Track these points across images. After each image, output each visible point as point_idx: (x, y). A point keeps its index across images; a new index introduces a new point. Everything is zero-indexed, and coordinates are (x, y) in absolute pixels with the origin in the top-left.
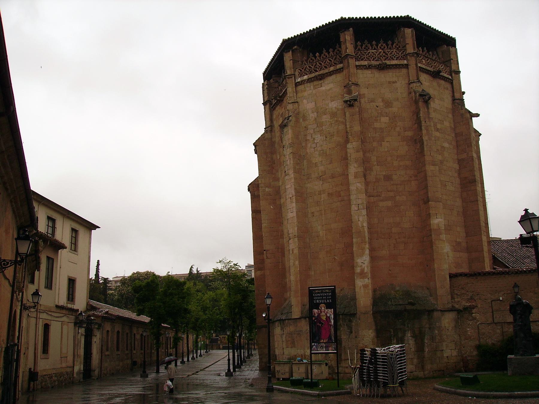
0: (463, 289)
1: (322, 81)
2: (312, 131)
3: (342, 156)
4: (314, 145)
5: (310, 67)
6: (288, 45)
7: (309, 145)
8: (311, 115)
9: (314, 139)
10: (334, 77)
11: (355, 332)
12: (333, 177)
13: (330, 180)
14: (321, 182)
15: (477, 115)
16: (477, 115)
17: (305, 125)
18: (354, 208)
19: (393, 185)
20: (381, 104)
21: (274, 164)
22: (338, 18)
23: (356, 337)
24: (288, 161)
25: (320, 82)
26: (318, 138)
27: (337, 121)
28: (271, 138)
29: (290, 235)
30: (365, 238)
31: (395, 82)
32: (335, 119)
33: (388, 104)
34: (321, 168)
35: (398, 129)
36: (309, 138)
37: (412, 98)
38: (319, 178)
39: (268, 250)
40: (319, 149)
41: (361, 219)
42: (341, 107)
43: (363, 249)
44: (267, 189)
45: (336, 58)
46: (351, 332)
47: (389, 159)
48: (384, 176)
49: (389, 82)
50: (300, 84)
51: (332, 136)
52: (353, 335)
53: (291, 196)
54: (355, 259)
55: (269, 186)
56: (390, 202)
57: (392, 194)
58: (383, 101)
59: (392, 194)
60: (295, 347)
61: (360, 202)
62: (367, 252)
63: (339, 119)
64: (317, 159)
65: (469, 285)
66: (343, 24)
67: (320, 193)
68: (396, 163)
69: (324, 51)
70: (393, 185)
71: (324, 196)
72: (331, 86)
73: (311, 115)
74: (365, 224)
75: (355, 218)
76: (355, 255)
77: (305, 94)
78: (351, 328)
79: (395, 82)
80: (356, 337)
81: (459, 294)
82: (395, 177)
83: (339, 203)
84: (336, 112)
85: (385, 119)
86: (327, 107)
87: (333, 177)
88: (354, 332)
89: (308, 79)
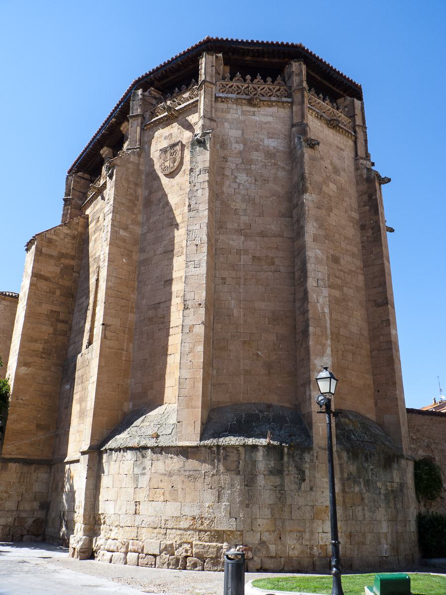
0: (418, 431)
1: (256, 109)
2: (233, 166)
3: (280, 212)
4: (236, 186)
5: (238, 87)
6: (210, 46)
7: (227, 183)
8: (234, 145)
9: (236, 177)
10: (274, 109)
11: (310, 481)
12: (262, 234)
13: (258, 238)
14: (243, 238)
15: (392, 230)
16: (392, 230)
17: (223, 155)
18: (311, 283)
19: (341, 270)
20: (330, 167)
21: (138, 201)
22: (296, 42)
23: (311, 489)
24: (200, 191)
25: (252, 109)
26: (242, 177)
27: (275, 164)
28: (138, 164)
29: (189, 303)
30: (325, 327)
31: (343, 150)
32: (273, 161)
33: (336, 171)
34: (244, 219)
35: (345, 204)
36: (228, 172)
37: (361, 175)
38: (239, 232)
39: (109, 326)
40: (243, 192)
41: (321, 300)
42: (282, 149)
43: (324, 345)
44: (122, 232)
45: (279, 90)
46: (304, 480)
47: (337, 236)
48: (332, 255)
49: (337, 147)
50: (222, 102)
51: (266, 181)
52: (305, 486)
53: (198, 243)
54: (312, 357)
55: (126, 229)
56: (338, 292)
57: (339, 282)
58: (331, 163)
59: (339, 282)
60: (175, 500)
61: (320, 276)
62: (329, 351)
63: (279, 163)
64: (238, 204)
65: (425, 427)
66: (296, 52)
67: (239, 252)
68: (343, 245)
69: (259, 77)
70: (341, 270)
71: (245, 259)
72: (270, 119)
73: (234, 145)
74: (327, 310)
75: (313, 296)
76: (311, 354)
77: (229, 116)
78: (304, 472)
79: (343, 150)
80: (311, 489)
81: (414, 438)
82: (342, 262)
83: (271, 273)
84: (275, 154)
85: (332, 186)
86: (261, 143)
87: (262, 234)
88: (307, 481)
89: (237, 99)
